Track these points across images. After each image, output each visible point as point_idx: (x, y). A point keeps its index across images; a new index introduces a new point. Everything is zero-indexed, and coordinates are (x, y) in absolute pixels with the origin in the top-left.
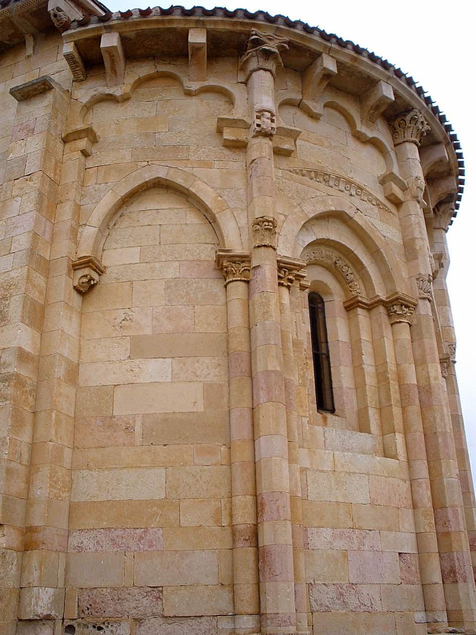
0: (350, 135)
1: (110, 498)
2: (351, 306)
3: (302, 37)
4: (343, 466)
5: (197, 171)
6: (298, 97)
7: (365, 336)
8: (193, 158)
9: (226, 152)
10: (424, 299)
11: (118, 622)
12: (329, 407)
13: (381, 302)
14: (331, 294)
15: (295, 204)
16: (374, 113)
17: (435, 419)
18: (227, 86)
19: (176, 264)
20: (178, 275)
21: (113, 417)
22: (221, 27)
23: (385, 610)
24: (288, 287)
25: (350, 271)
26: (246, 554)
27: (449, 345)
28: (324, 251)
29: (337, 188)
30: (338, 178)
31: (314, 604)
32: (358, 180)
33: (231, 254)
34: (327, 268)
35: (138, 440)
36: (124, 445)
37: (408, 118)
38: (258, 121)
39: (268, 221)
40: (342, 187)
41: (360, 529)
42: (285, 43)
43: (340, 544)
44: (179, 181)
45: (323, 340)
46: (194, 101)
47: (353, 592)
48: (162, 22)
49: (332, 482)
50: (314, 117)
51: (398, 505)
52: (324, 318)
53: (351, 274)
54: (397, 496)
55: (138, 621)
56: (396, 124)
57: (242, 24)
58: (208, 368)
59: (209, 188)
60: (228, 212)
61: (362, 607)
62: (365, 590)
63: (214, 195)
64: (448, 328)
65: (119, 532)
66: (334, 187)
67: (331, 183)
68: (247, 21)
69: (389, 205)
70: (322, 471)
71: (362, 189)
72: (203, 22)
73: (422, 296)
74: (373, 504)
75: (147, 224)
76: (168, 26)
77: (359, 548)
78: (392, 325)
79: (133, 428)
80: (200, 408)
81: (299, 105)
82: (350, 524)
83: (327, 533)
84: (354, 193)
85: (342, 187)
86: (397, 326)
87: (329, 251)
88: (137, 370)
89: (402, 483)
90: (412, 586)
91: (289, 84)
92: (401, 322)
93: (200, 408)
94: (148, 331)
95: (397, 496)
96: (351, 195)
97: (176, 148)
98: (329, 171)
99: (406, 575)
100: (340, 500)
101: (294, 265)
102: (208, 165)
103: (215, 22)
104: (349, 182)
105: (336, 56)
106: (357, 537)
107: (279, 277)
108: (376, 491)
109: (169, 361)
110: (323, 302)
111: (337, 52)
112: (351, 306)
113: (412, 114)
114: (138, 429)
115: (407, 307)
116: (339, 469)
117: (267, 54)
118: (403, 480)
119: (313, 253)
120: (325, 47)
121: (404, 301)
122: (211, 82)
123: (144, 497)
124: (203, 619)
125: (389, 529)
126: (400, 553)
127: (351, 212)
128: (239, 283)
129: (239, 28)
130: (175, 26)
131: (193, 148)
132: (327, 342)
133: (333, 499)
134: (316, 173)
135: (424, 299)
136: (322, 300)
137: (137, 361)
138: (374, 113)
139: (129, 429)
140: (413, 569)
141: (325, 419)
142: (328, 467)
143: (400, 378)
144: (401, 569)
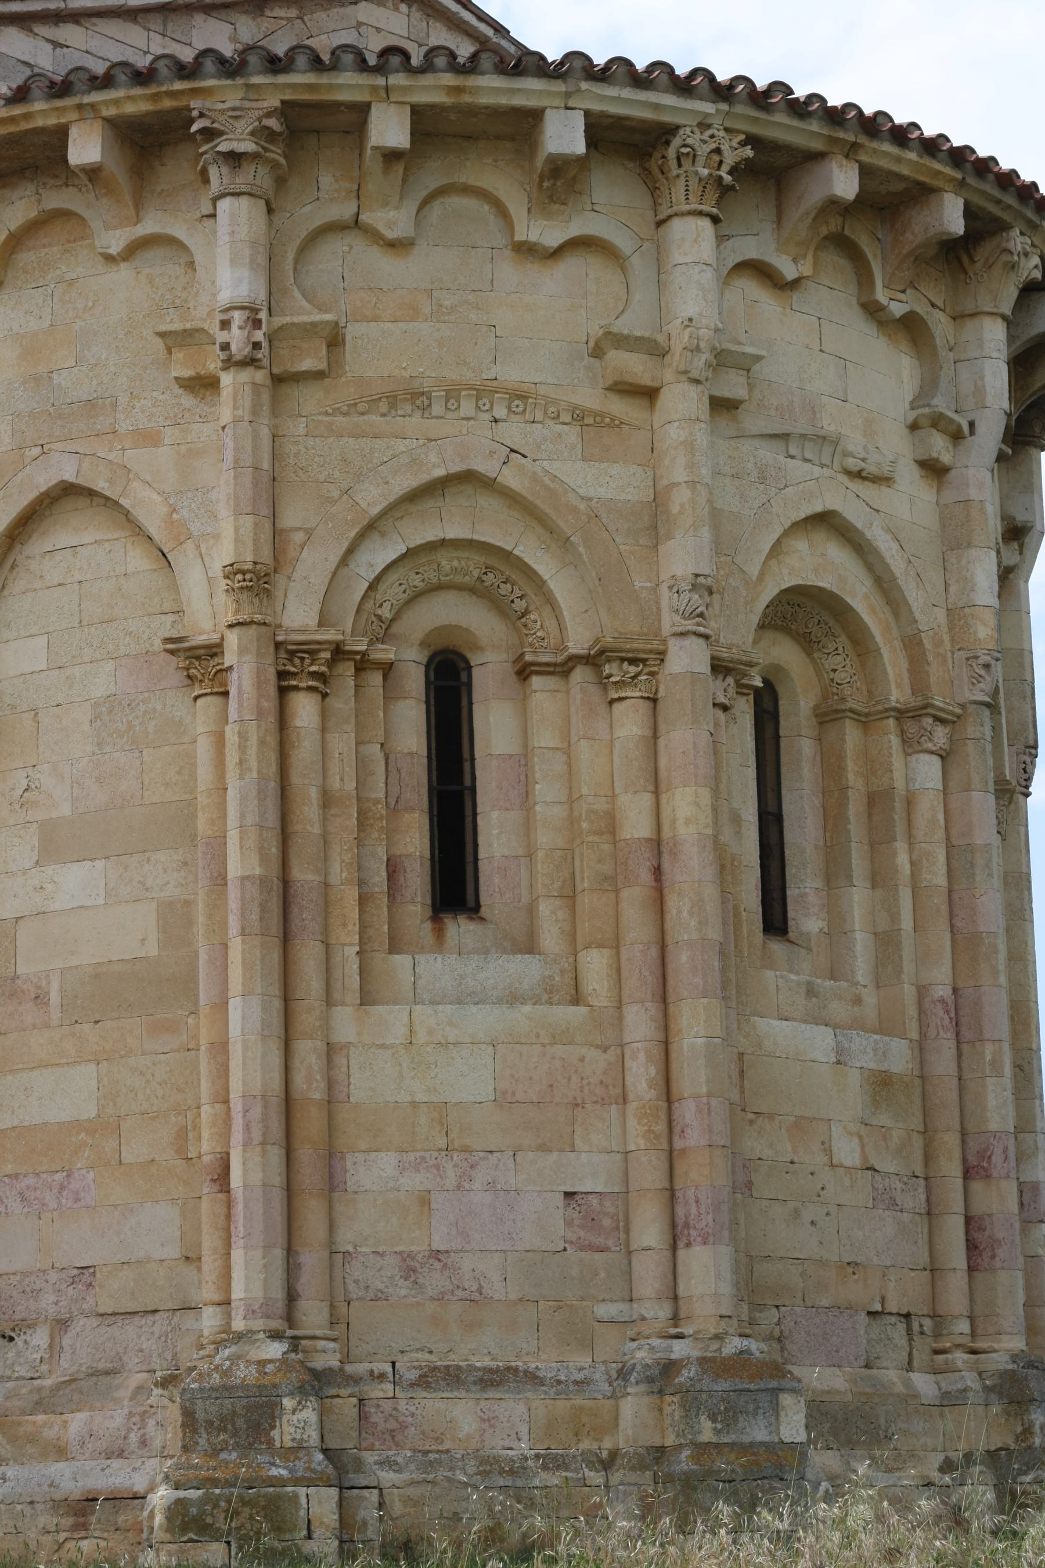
0: (508, 252)
1: (16, 1123)
2: (524, 672)
3: (311, 87)
4: (430, 1032)
5: (135, 457)
6: (345, 211)
7: (545, 738)
8: (124, 427)
9: (187, 400)
10: (682, 634)
11: (32, 1326)
12: (471, 902)
13: (575, 660)
14: (481, 649)
15: (336, 494)
16: (554, 184)
17: (680, 912)
18: (179, 232)
19: (110, 666)
20: (113, 689)
21: (15, 977)
22: (130, 109)
23: (513, 1296)
24: (310, 689)
25: (518, 592)
26: (209, 1205)
27: (968, 659)
28: (446, 561)
29: (455, 415)
30: (452, 394)
31: (351, 1287)
32: (511, 374)
33: (186, 645)
34: (472, 590)
35: (55, 1014)
36: (34, 1027)
37: (671, 153)
38: (221, 337)
39: (244, 572)
40: (467, 407)
41: (466, 1149)
42: (268, 115)
43: (415, 1181)
44: (101, 485)
45: (466, 754)
46: (124, 272)
47: (438, 1265)
48: (12, 120)
49: (404, 1065)
50: (398, 246)
51: (575, 1098)
52: (470, 704)
53: (521, 598)
54: (575, 1080)
55: (62, 1324)
56: (654, 165)
57: (172, 94)
58: (165, 871)
59: (155, 496)
60: (189, 545)
61: (459, 1293)
62: (467, 1263)
63: (164, 510)
64: (967, 610)
65: (31, 1181)
66: (450, 415)
67: (437, 409)
68: (179, 86)
69: (619, 407)
70: (382, 1046)
71: (523, 398)
72: (92, 106)
73: (680, 629)
74: (503, 1100)
75: (56, 583)
76: (25, 126)
77: (458, 1188)
78: (611, 702)
79: (48, 993)
80: (152, 950)
81: (356, 224)
82: (442, 1143)
83: (387, 1162)
84: (500, 412)
85: (467, 407)
86: (616, 706)
87: (459, 559)
88: (49, 887)
89: (592, 1054)
90: (597, 1256)
91: (326, 180)
92: (621, 699)
93: (152, 950)
94: (65, 810)
95: (575, 1080)
96: (496, 421)
97: (90, 405)
98: (426, 385)
99: (582, 1233)
100: (420, 1097)
101: (319, 643)
102: (149, 438)
103: (116, 102)
104: (483, 393)
105: (407, 99)
106: (455, 1166)
107: (282, 675)
108: (512, 1076)
109: (100, 864)
110: (469, 668)
111: (406, 89)
112: (524, 672)
113: (676, 142)
114: (55, 997)
115: (633, 661)
116: (421, 1037)
117: (234, 159)
118: (597, 1047)
119: (417, 573)
120: (374, 89)
121: (614, 651)
122: (148, 227)
123: (64, 1117)
124: (157, 1316)
125: (543, 1148)
126: (569, 1195)
127: (486, 467)
128: (209, 698)
129: (167, 104)
130: (40, 122)
131: (123, 400)
132: (473, 759)
133: (404, 1097)
134: (393, 401)
135: (682, 634)
136: (467, 662)
137: (49, 870)
138: (554, 184)
139: (40, 999)
140: (607, 1222)
141: (439, 933)
142: (398, 1033)
143: (610, 824)
144: (569, 1223)
